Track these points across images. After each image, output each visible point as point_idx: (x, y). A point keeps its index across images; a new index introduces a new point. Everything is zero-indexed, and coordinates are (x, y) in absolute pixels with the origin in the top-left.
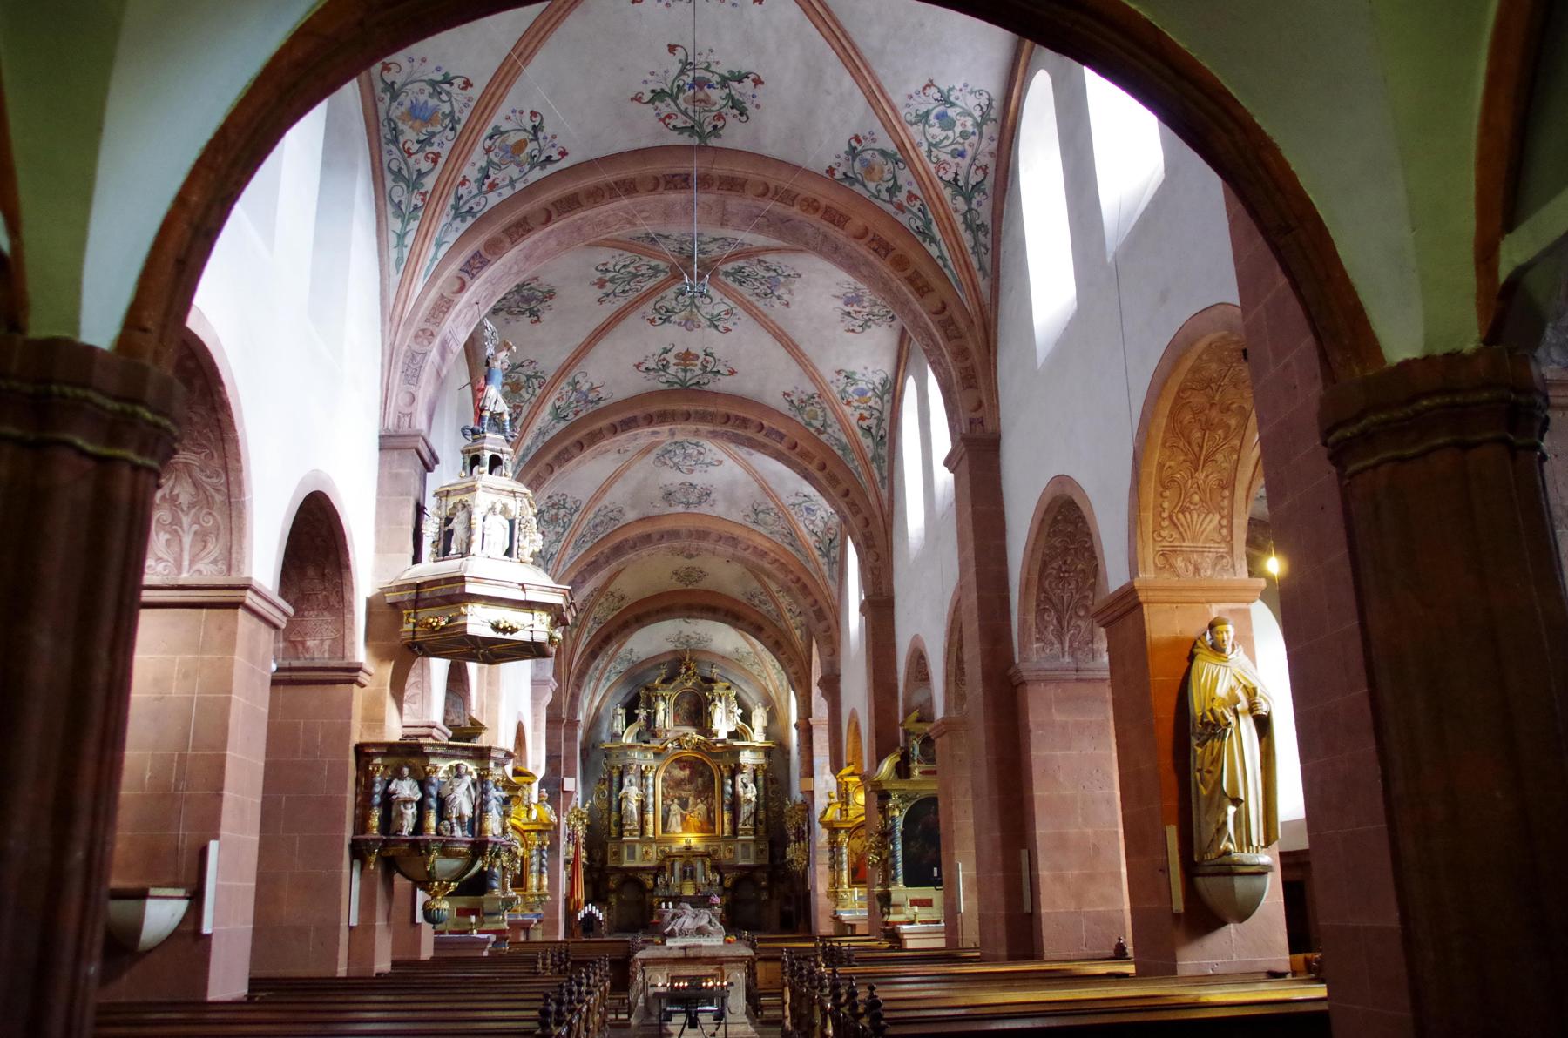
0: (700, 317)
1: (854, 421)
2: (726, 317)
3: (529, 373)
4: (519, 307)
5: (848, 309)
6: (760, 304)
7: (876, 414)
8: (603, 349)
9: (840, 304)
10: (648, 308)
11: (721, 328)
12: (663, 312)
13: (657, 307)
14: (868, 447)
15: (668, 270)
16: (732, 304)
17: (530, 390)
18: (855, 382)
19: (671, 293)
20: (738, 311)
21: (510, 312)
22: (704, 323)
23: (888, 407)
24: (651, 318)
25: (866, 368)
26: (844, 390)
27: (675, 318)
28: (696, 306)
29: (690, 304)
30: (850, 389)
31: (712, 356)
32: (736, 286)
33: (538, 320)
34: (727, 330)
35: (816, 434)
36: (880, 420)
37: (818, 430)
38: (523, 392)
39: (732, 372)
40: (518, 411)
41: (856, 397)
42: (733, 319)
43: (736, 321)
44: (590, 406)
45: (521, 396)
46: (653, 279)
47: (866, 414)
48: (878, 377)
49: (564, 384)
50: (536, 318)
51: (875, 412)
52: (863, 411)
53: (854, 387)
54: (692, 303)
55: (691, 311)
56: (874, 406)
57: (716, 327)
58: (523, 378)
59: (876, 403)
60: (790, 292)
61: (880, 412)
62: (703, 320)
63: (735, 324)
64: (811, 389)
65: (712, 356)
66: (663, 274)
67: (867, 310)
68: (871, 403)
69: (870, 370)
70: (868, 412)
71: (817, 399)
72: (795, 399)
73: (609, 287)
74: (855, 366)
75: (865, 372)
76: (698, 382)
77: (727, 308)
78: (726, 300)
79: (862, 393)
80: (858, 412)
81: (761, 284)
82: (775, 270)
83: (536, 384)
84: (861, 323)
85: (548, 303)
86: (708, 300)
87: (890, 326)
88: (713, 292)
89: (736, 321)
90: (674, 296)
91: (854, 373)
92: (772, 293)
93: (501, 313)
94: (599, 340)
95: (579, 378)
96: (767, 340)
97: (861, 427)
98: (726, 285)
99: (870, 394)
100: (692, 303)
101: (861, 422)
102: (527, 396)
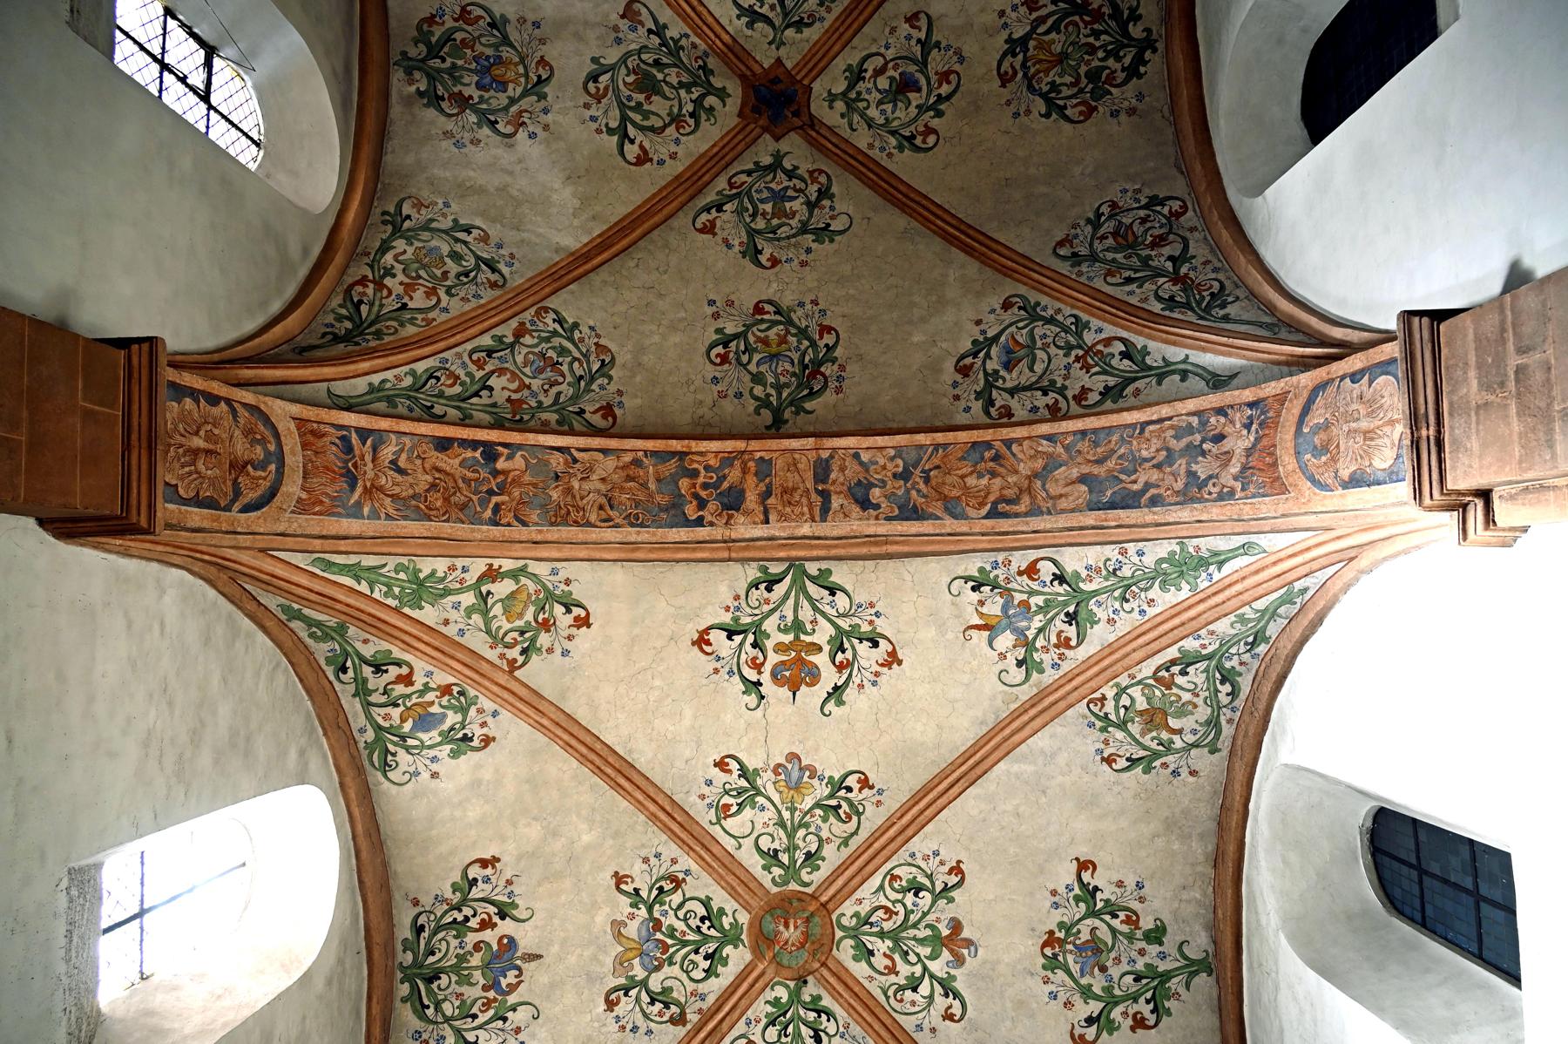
0: (776, 798)
1: (420, 666)
2: (727, 800)
3: (1120, 735)
4: (1113, 931)
5: (506, 927)
6: (671, 849)
7: (376, 698)
8: (964, 731)
9: (527, 937)
10: (873, 818)
11: (734, 766)
12: (845, 806)
13: (855, 819)
14: (366, 641)
15: (839, 934)
16: (716, 831)
17: (1125, 701)
18: (447, 737)
19: (832, 856)
20: (705, 816)
21: (1133, 920)
22: (766, 781)
23: (358, 719)
24: (866, 792)
25: (435, 775)
26: (464, 710)
27: (822, 790)
28: (781, 823)
29: (795, 830)
30: (452, 718)
31: (744, 679)
32: (721, 899)
33: (1084, 865)
34: (721, 765)
35: (496, 563)
36: (362, 690)
37: (492, 575)
38: (1141, 704)
39: (702, 641)
40: (1163, 673)
41: (435, 709)
42: (712, 793)
43: (706, 790)
44: (1000, 573)
45: (1149, 700)
46: (864, 909)
47: (400, 689)
48: (403, 767)
49: (1050, 676)
50: (1086, 877)
51: (383, 699)
52: (410, 690)
53: (446, 727)
54: (791, 836)
55: (792, 810)
56: (389, 710)
57: (744, 773)
58: (1135, 728)
59: (387, 717)
60: (617, 926)
61: (370, 704)
62: (771, 791)
63: (709, 783)
64: (537, 672)
65: (744, 679)
66: (845, 921)
67: (471, 938)
68: (396, 713)
69: (425, 775)
70: (395, 694)
71: (514, 653)
72: (564, 620)
73: (943, 915)
74: (458, 771)
75: (435, 767)
76: (771, 583)
77: (729, 824)
78: (729, 843)
79: (425, 721)
80: (418, 686)
81: (672, 932)
82: (652, 1002)
83: (1110, 707)
84: (476, 893)
85: (1057, 916)
86: (765, 843)
87: (416, 903)
88: (754, 863)
89: (706, 790)
90: (828, 851)
91: (455, 754)
92: (650, 909)
93: (1147, 923)
94: (966, 756)
95: (1017, 675)
96: (644, 757)
97: (398, 664)
98: (734, 894)
99: (407, 727)
100: (791, 836)
101: (405, 670)
102: (1136, 692)
